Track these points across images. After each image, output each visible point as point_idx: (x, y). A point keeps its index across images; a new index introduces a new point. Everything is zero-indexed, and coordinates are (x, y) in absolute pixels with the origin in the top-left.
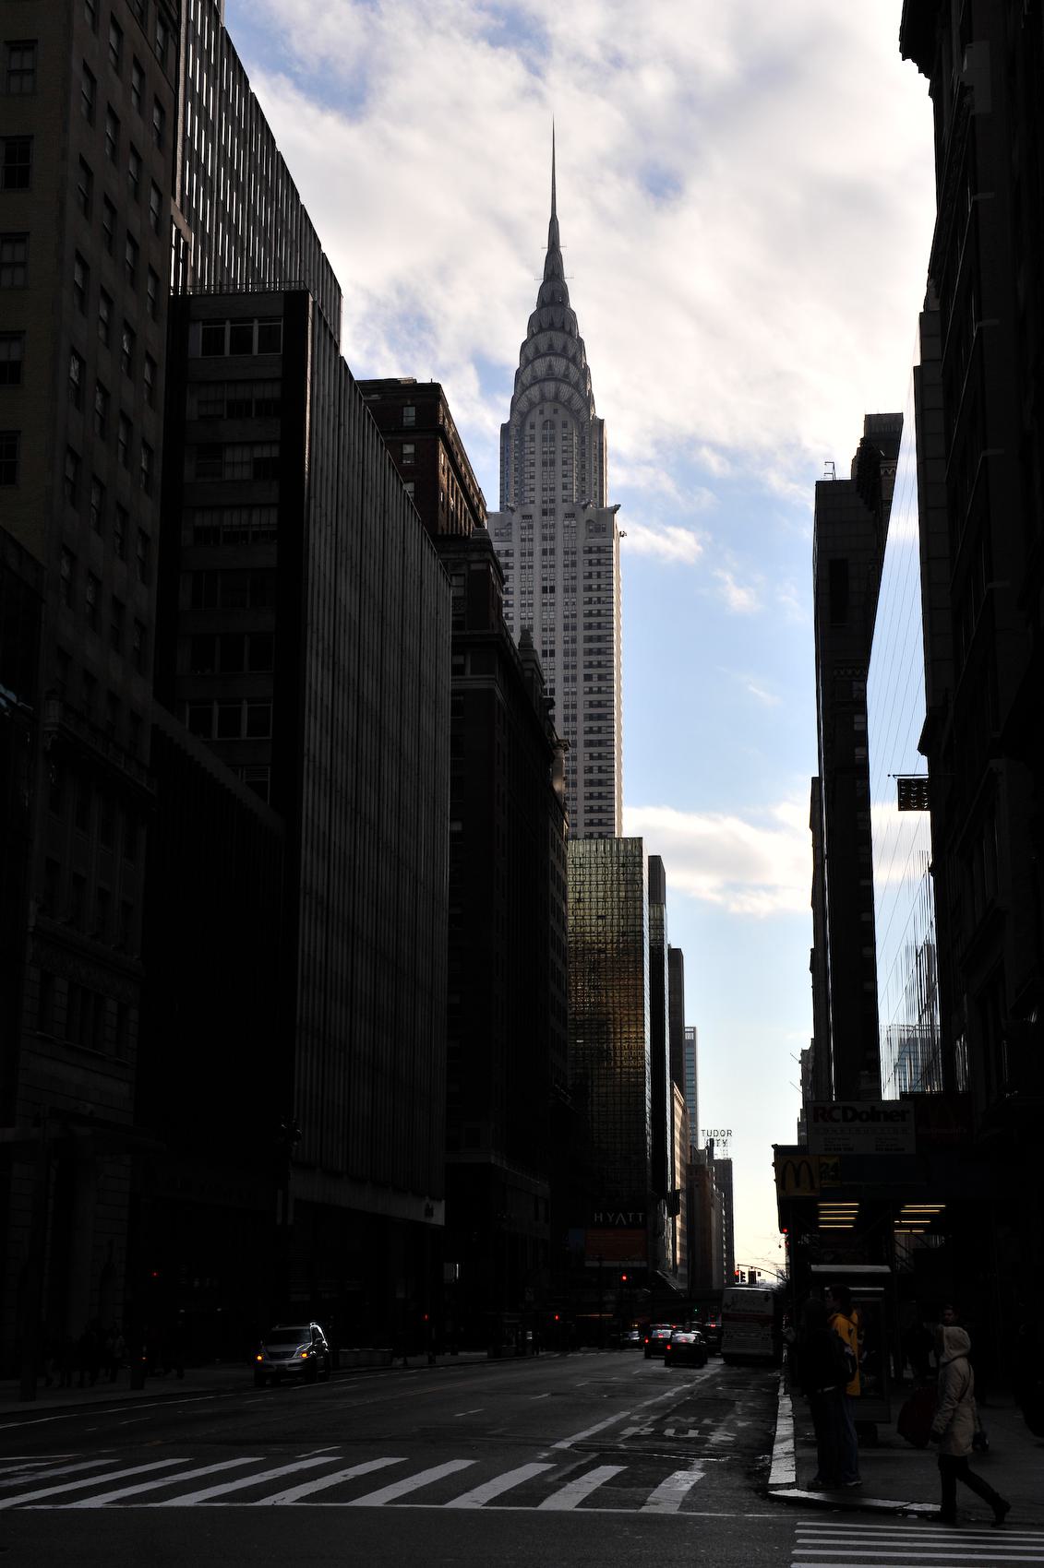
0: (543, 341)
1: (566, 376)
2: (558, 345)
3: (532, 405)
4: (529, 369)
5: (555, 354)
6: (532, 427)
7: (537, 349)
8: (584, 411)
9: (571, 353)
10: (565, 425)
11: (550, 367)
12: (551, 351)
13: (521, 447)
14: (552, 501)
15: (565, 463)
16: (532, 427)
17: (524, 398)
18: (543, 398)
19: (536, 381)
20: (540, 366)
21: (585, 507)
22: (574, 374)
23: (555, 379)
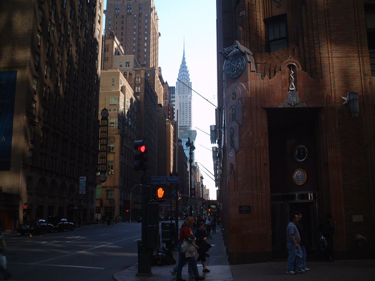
0: (182, 69)
2: (185, 70)
5: (184, 72)
8: (189, 81)
9: (187, 71)
11: (184, 74)
12: (184, 71)
20: (182, 73)
22: (187, 75)
23: (184, 76)
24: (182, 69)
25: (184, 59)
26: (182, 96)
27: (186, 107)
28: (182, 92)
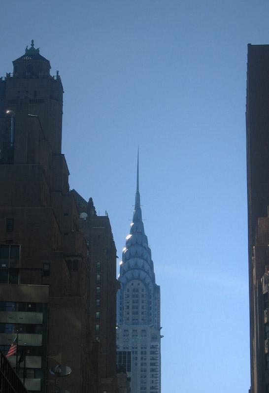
1: (143, 267)
4: (127, 262)
5: (139, 257)
8: (151, 285)
10: (143, 290)
11: (136, 264)
16: (128, 290)
19: (129, 268)
21: (151, 327)
22: (147, 267)
26: (131, 331)
27: (144, 361)
28: (130, 319)
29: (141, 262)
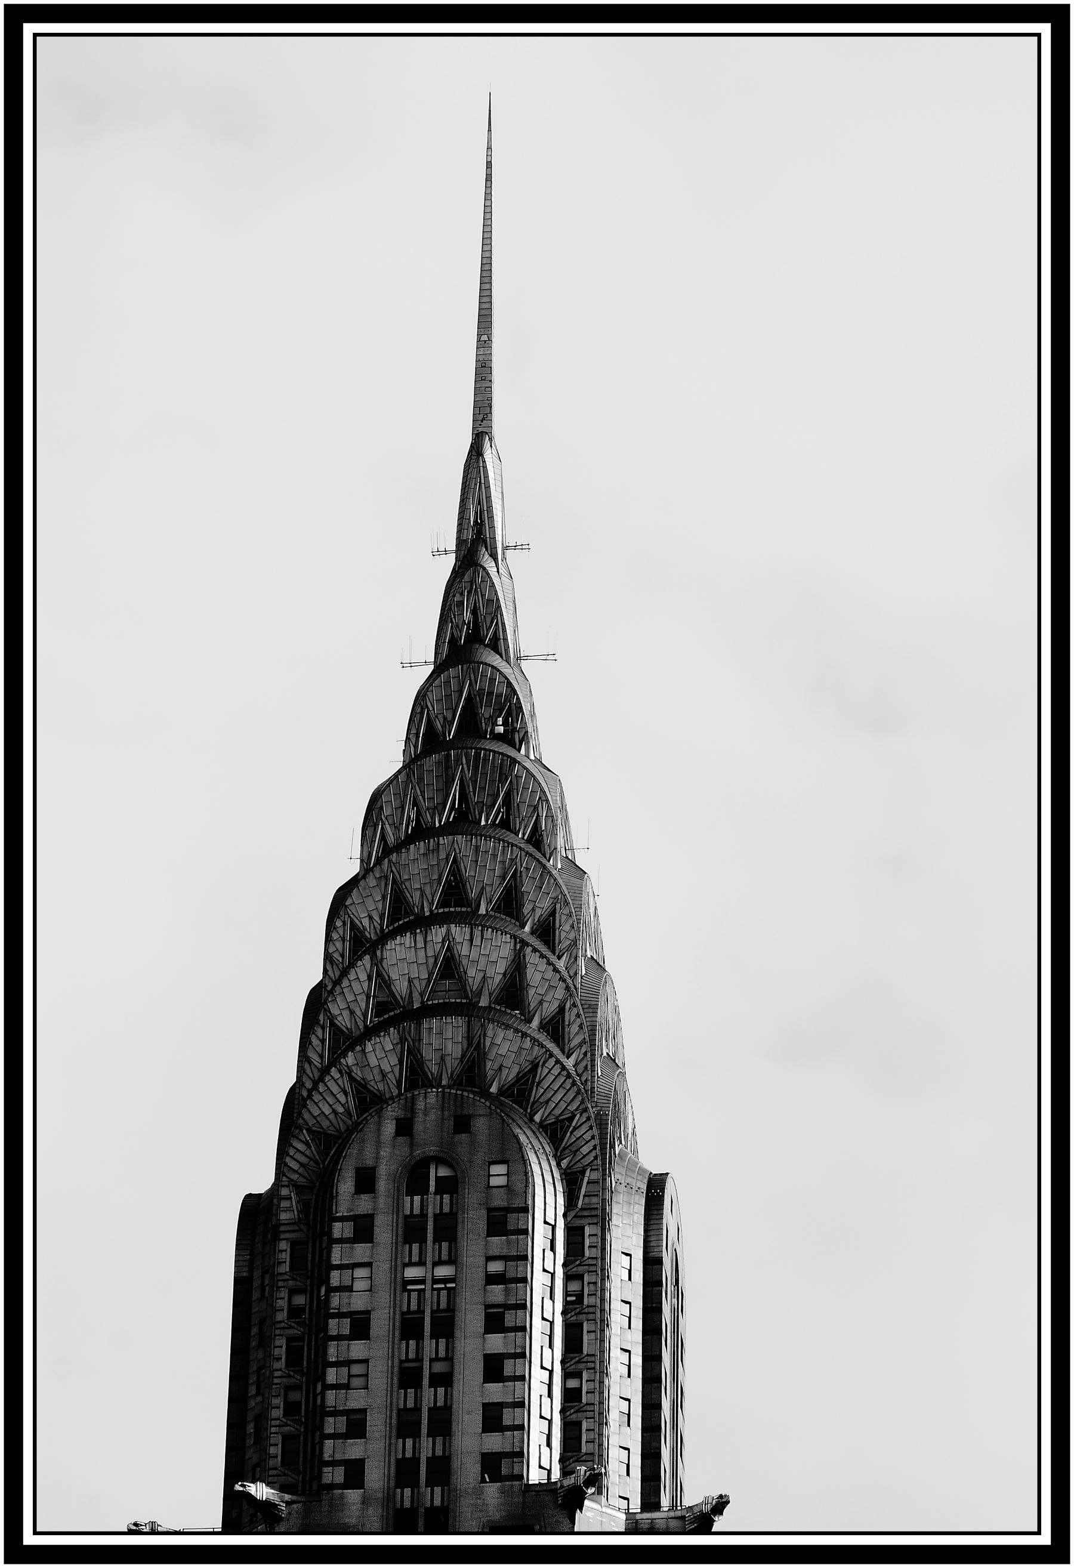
3: (368, 1100)
4: (363, 969)
5: (470, 918)
6: (366, 1182)
7: (399, 904)
11: (449, 967)
13: (312, 1267)
14: (442, 1470)
15: (494, 1322)
16: (366, 1182)
17: (335, 1082)
18: (416, 1075)
20: (407, 961)
23: (466, 1008)
24: (420, 873)
25: (471, 629)
29: (487, 956)
